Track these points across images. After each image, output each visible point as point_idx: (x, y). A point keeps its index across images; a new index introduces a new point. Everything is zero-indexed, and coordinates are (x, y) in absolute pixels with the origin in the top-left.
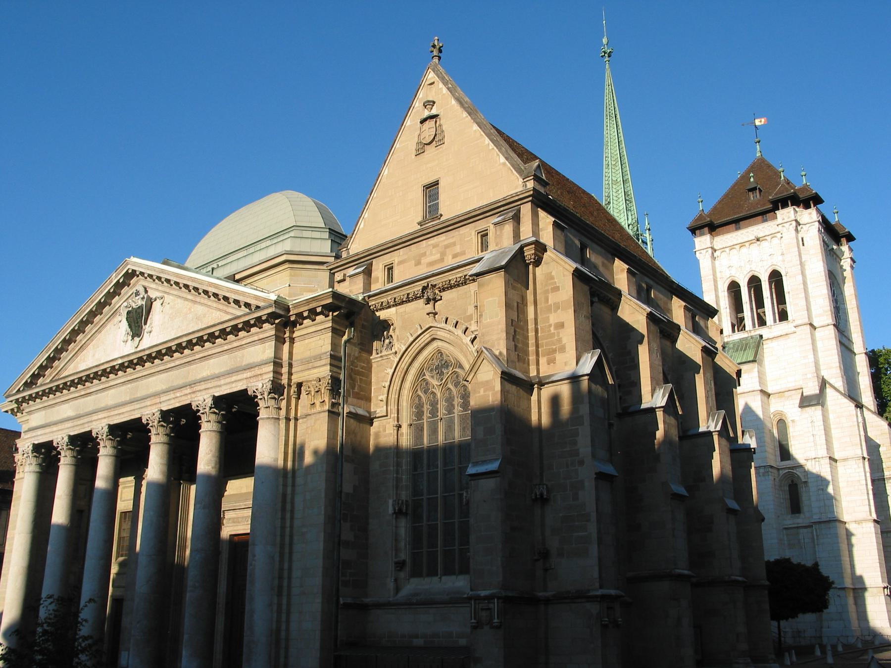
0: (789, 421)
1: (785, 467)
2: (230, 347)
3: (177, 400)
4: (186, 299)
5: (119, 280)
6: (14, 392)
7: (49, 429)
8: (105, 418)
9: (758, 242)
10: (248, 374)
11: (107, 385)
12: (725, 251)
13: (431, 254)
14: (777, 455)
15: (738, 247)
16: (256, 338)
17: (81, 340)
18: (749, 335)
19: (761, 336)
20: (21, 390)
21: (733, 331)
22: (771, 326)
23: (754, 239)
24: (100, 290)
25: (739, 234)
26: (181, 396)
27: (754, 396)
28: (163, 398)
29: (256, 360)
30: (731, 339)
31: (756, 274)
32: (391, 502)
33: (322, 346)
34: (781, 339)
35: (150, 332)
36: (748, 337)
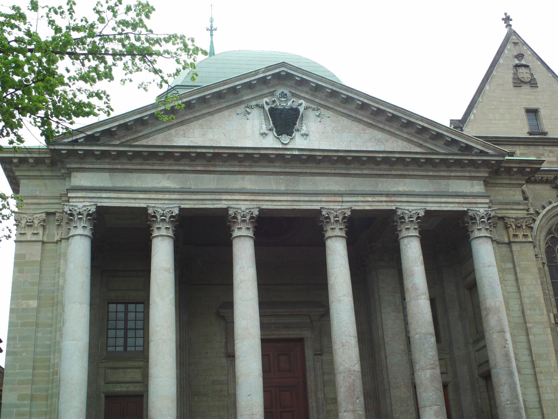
2: (436, 174)
3: (368, 204)
4: (360, 121)
5: (266, 76)
6: (66, 140)
7: (129, 195)
8: (246, 200)
10: (461, 200)
11: (248, 169)
13: (549, 156)
16: (467, 174)
17: (184, 115)
20: (80, 141)
24: (240, 77)
26: (374, 201)
28: (345, 199)
29: (465, 191)
32: (552, 315)
33: (514, 195)
35: (307, 135)
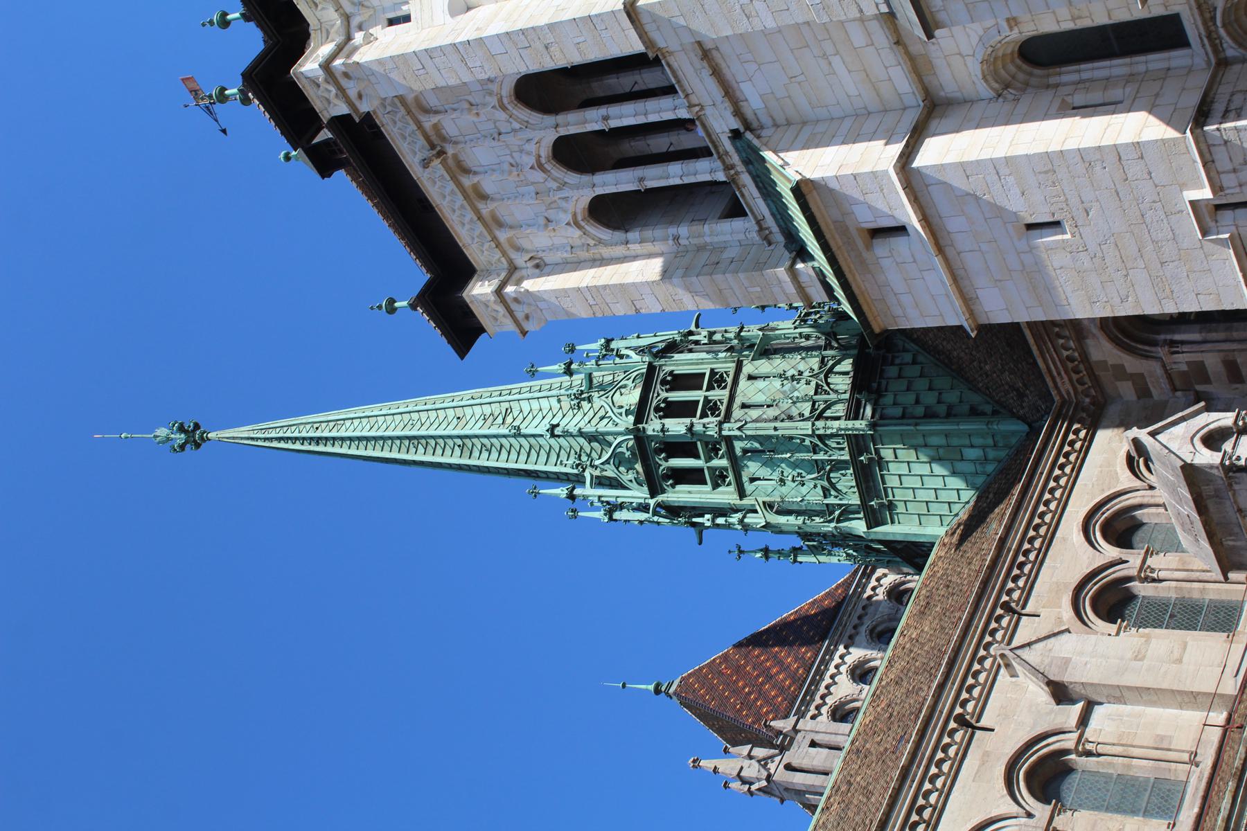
0: (1016, 35)
1: (1206, 41)
9: (450, 150)
12: (509, 241)
14: (1165, 65)
15: (485, 209)
18: (744, 170)
19: (736, 135)
21: (745, 214)
22: (690, 106)
23: (444, 163)
25: (445, 203)
27: (927, 186)
30: (770, 222)
31: (546, 151)
34: (729, 76)
36: (750, 173)
